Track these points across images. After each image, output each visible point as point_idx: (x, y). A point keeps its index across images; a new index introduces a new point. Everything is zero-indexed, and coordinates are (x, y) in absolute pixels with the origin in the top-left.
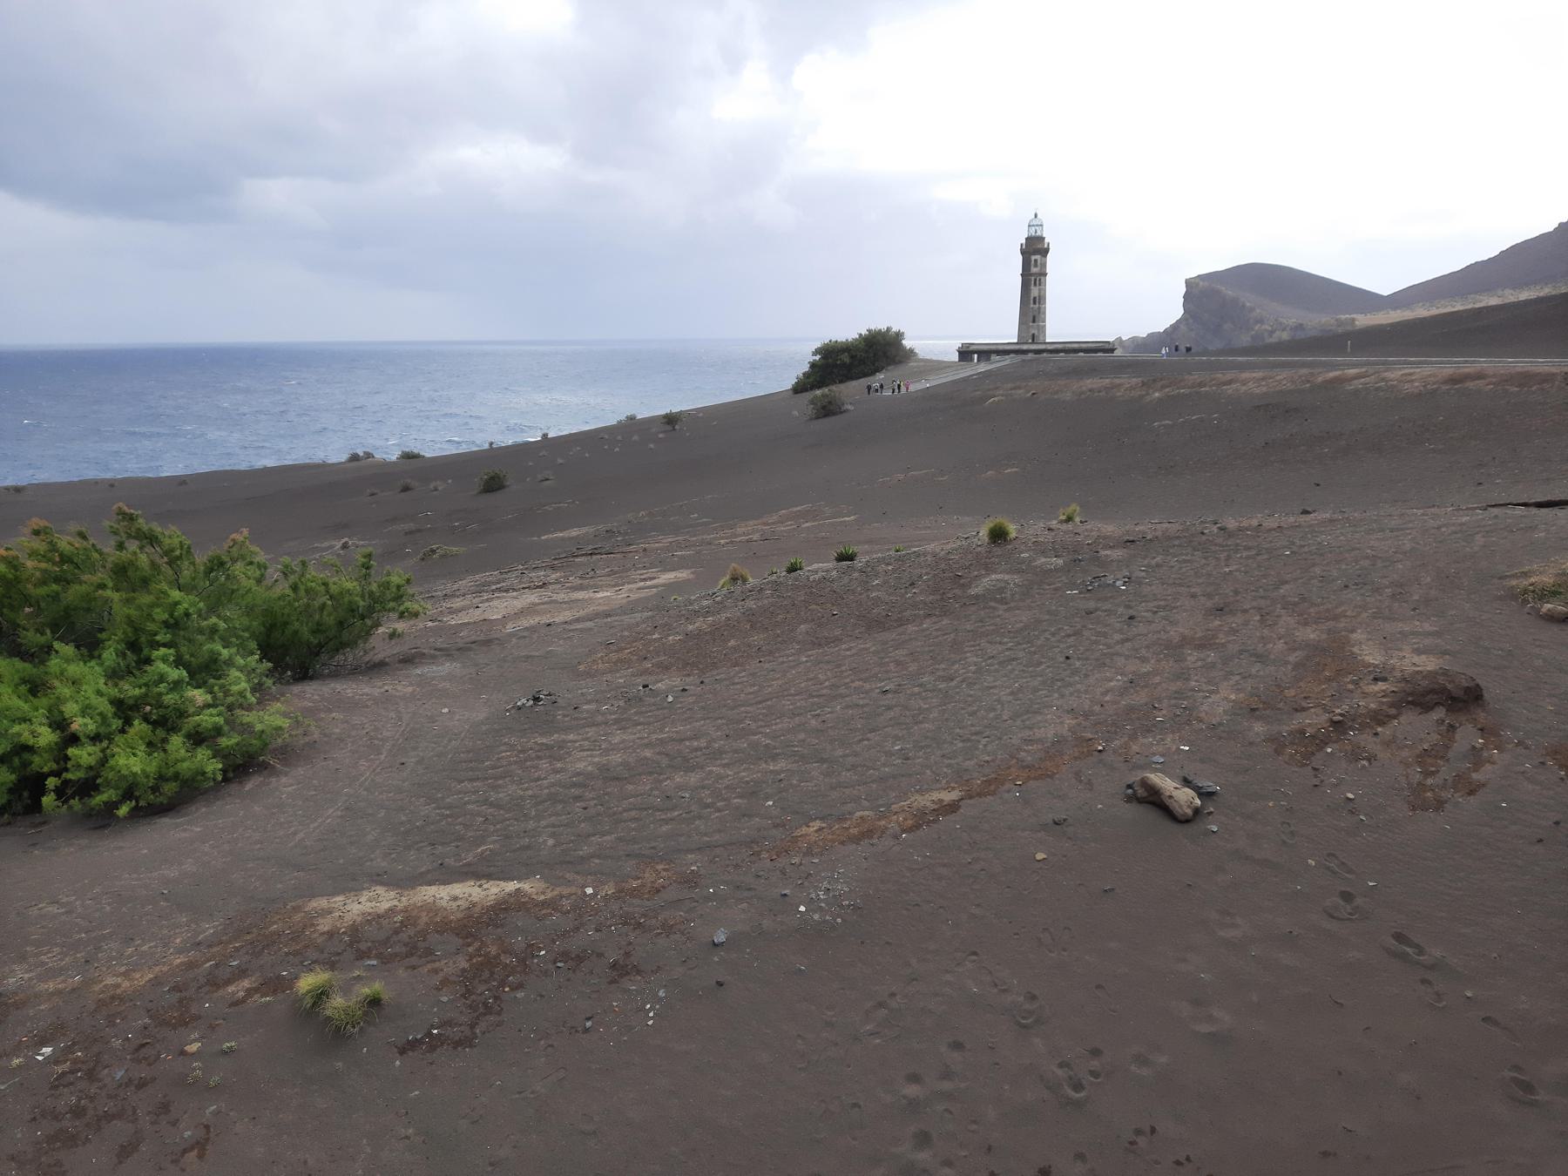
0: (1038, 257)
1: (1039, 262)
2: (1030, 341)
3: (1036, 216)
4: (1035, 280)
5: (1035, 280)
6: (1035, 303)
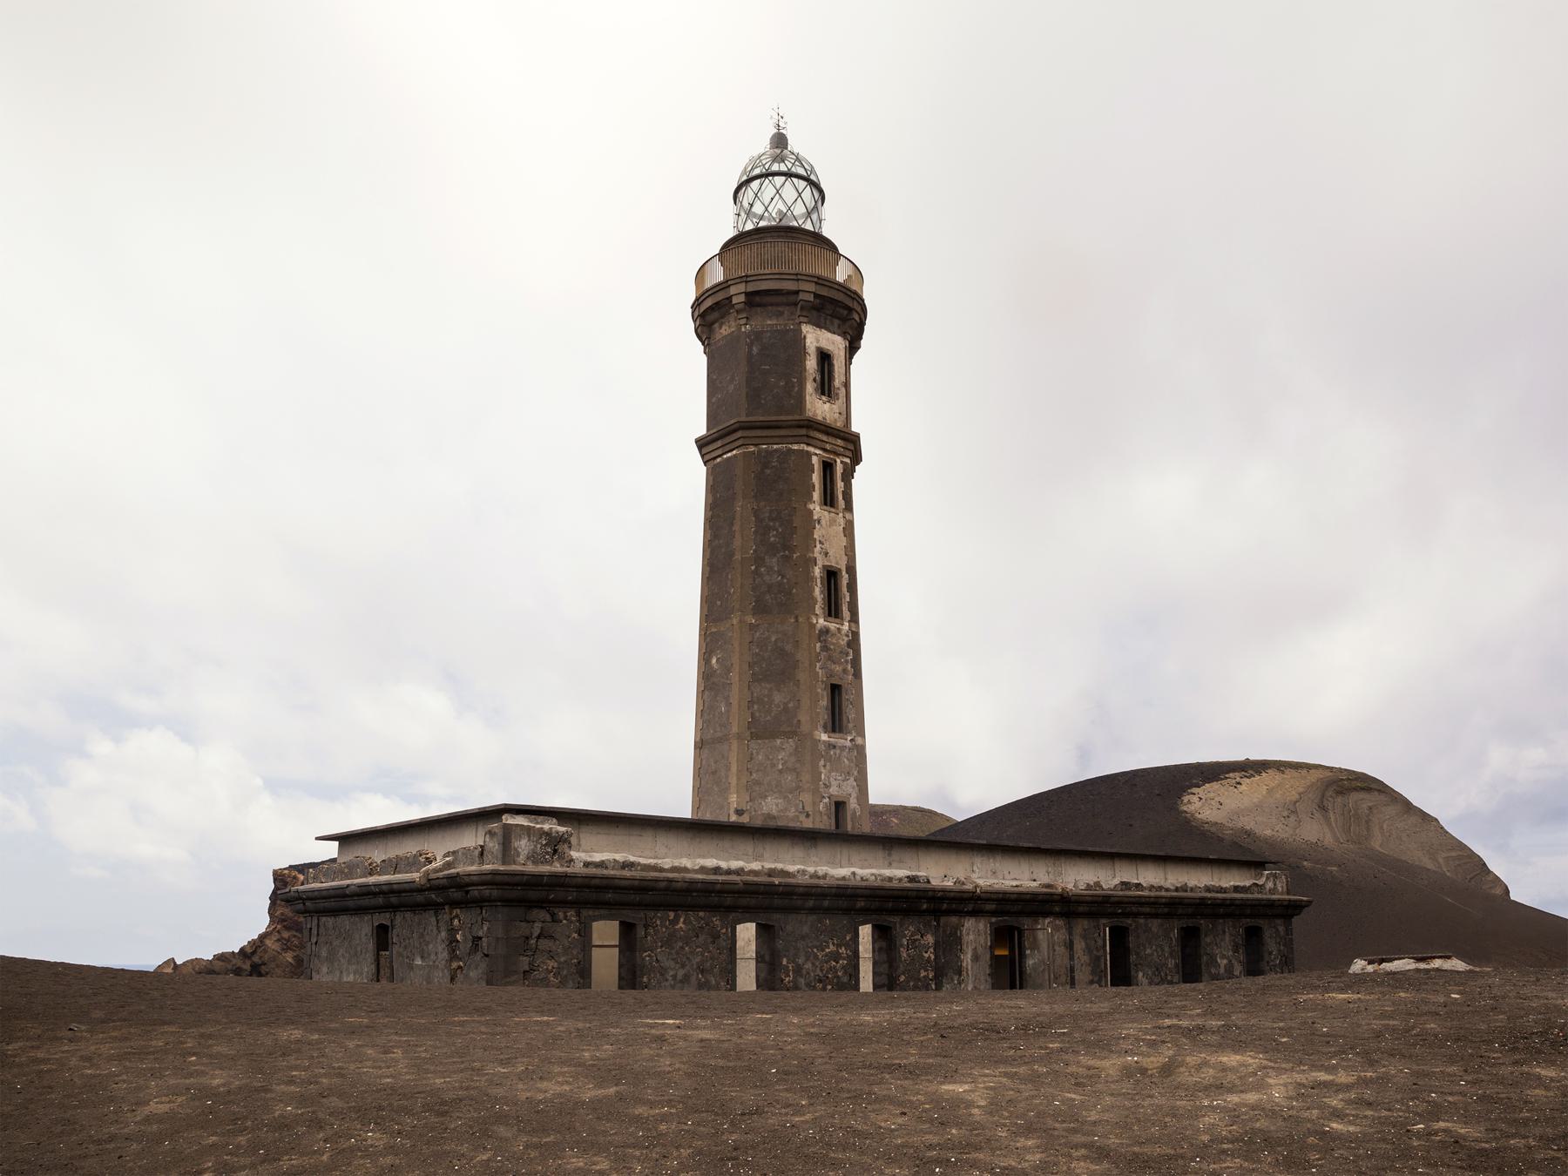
0: (834, 343)
3: (780, 141)
4: (828, 467)
5: (828, 467)
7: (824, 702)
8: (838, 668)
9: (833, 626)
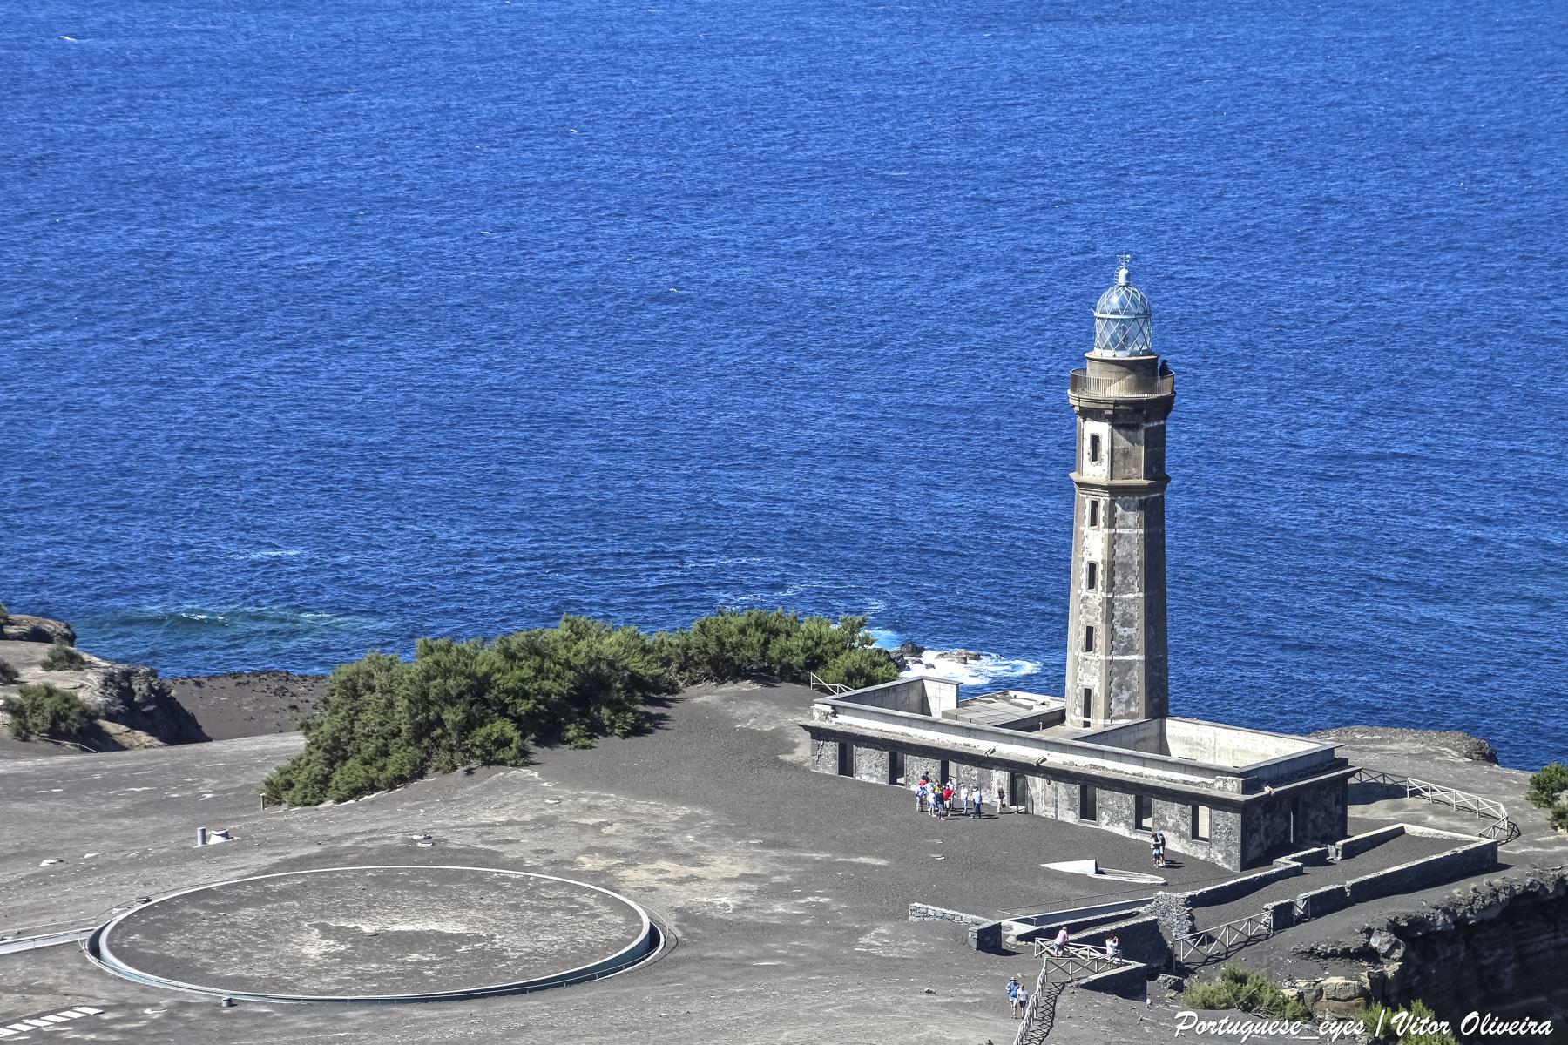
1: (1105, 446)
4: (1094, 505)
5: (1094, 505)
6: (1092, 584)
7: (1083, 636)
8: (1092, 618)
9: (1091, 593)
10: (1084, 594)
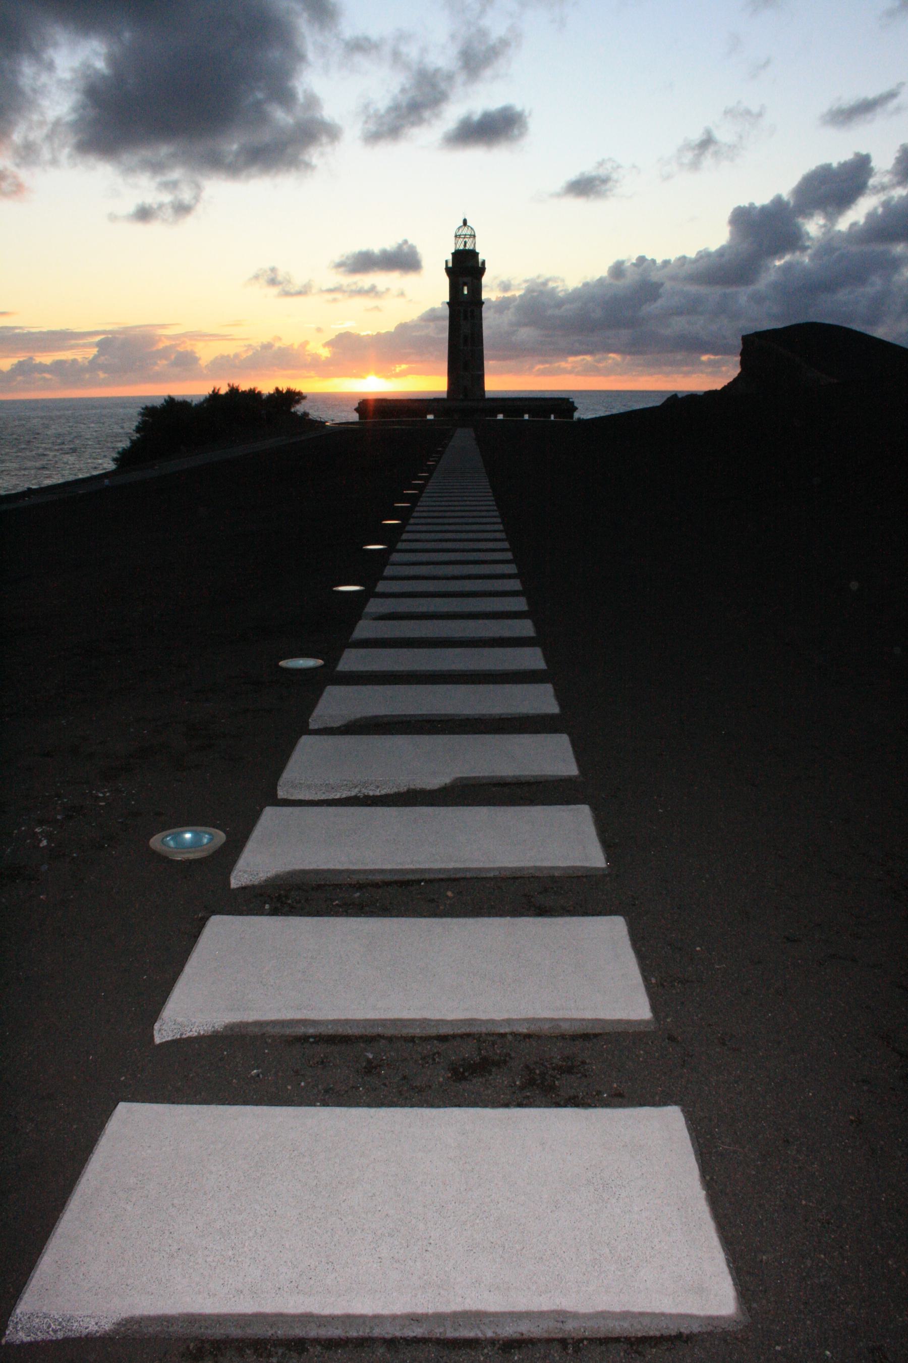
0: (467, 279)
2: (461, 396)
3: (465, 222)
10: (462, 348)
